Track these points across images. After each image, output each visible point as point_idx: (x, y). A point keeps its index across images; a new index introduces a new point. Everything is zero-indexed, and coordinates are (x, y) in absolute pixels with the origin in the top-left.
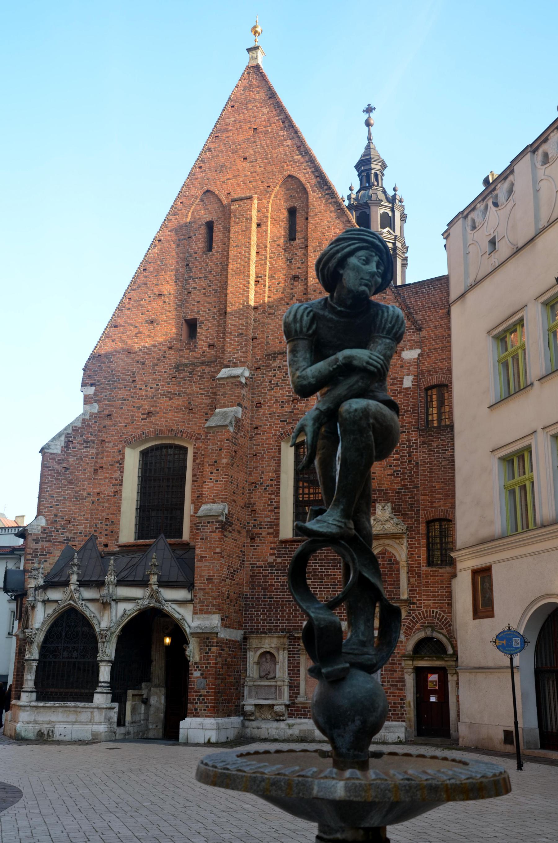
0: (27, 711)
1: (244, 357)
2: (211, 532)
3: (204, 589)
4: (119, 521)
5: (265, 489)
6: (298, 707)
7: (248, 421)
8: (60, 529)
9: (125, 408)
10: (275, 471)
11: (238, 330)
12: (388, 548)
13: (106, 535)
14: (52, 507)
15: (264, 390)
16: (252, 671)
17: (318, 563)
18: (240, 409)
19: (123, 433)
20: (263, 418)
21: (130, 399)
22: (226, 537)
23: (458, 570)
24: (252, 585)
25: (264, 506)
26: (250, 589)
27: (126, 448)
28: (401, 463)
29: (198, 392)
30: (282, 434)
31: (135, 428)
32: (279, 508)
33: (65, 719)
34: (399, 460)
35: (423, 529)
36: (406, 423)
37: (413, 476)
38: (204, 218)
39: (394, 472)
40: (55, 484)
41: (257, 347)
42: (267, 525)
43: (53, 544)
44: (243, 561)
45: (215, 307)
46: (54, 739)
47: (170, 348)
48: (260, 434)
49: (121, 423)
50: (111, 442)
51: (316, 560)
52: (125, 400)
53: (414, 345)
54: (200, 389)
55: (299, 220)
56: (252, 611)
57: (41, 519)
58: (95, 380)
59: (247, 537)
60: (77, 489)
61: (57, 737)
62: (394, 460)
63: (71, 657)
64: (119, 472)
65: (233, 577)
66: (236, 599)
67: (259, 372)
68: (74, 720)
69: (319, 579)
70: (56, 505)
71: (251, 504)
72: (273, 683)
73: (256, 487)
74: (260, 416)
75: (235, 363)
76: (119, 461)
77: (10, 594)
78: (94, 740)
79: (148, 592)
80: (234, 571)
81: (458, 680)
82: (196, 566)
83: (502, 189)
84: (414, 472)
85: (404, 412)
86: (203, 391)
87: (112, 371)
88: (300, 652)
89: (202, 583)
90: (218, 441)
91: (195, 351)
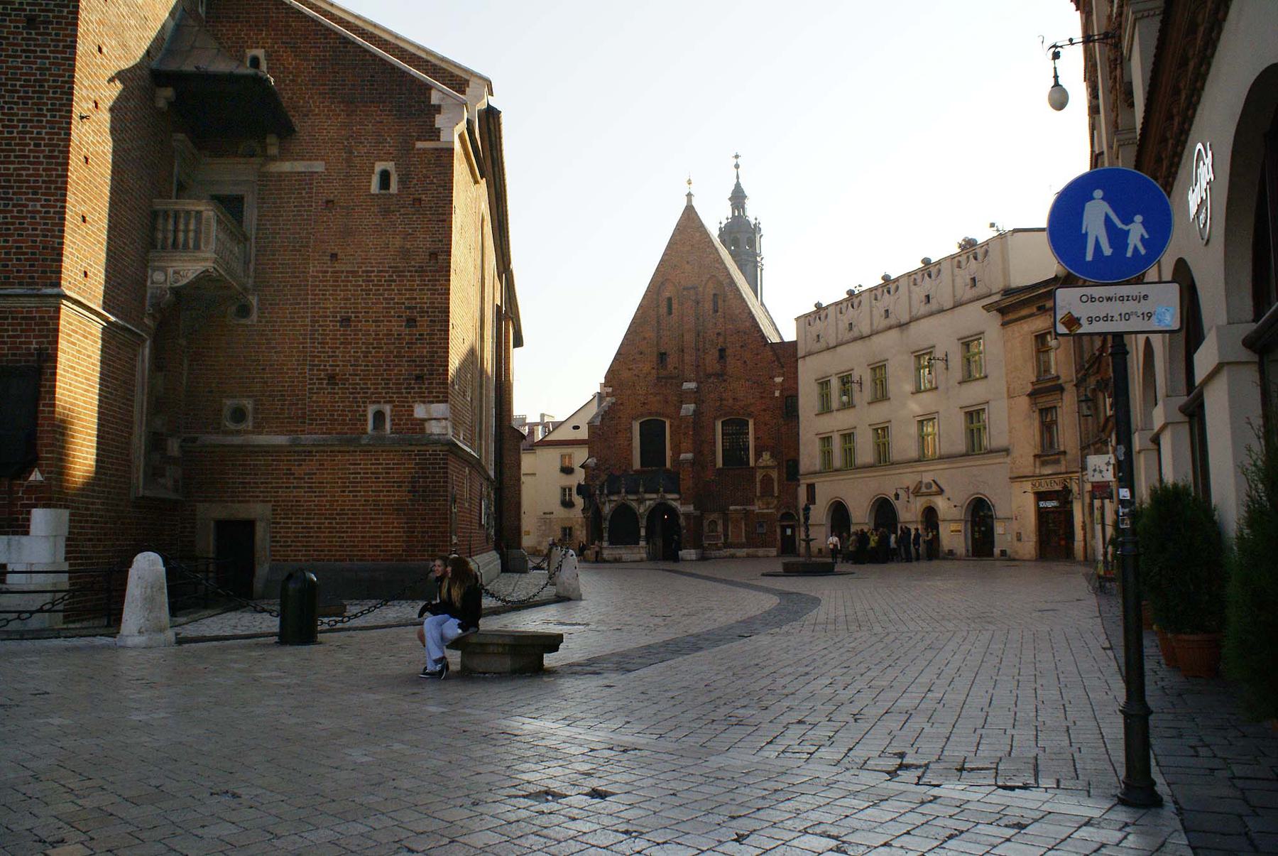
16: (706, 529)
35: (785, 465)
47: (653, 368)
55: (720, 302)
78: (642, 561)
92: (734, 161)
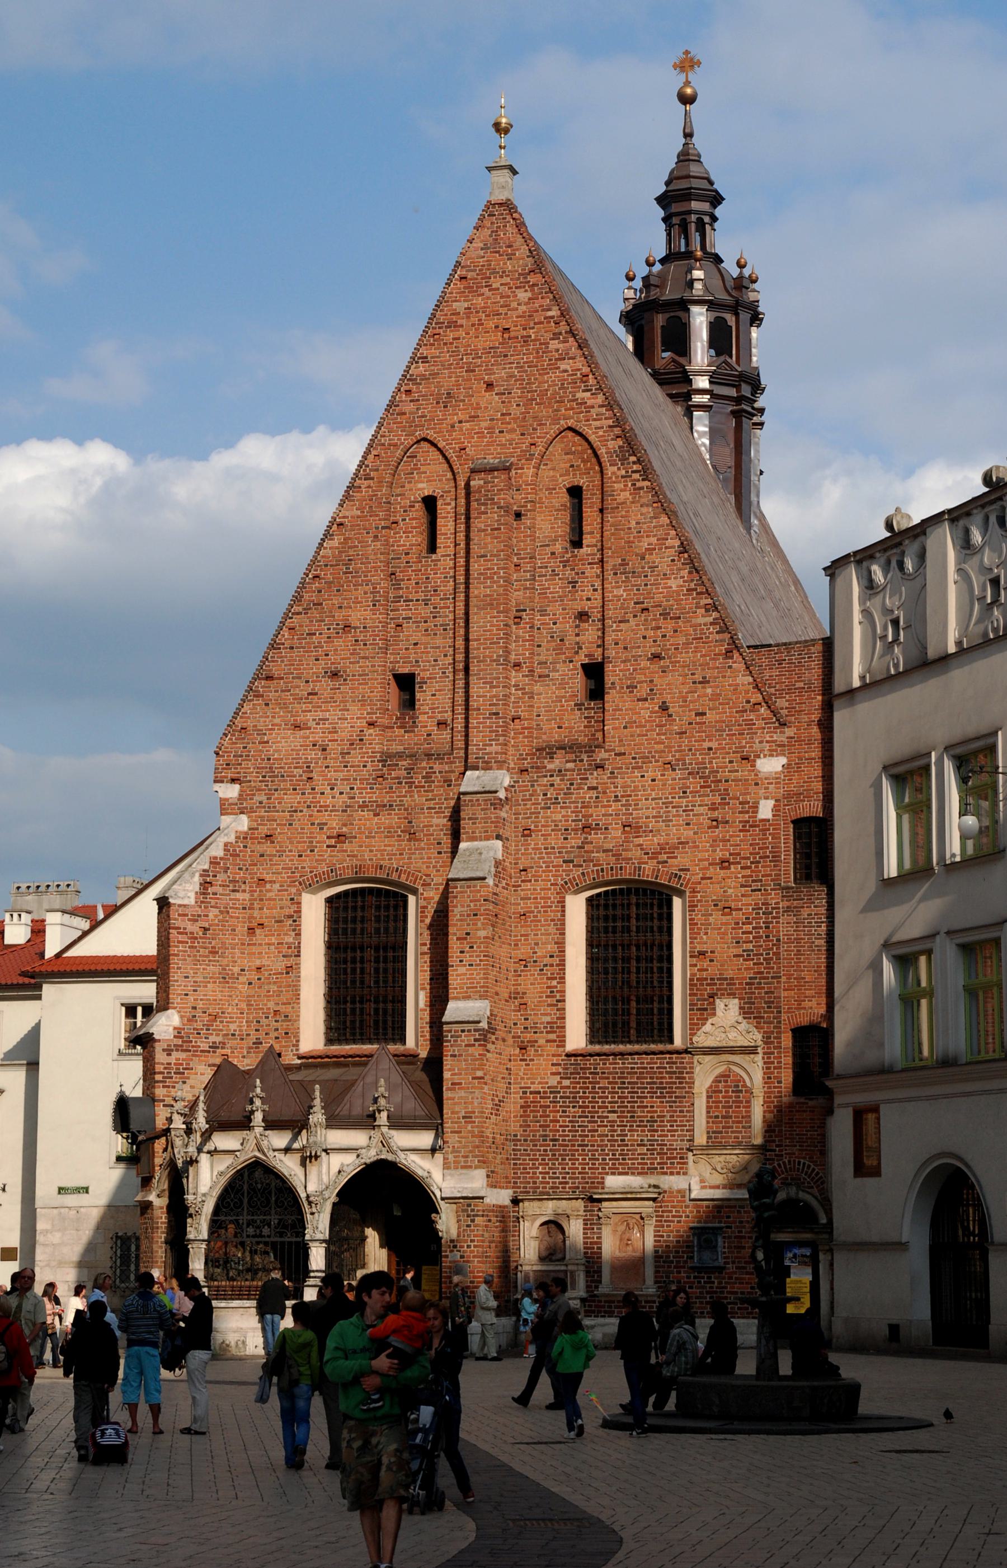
1: (502, 753)
2: (466, 1046)
3: (460, 1132)
4: (298, 1016)
5: (542, 970)
6: (600, 1301)
7: (511, 859)
9: (296, 824)
10: (556, 943)
11: (490, 705)
12: (734, 1068)
13: (277, 1038)
14: (187, 995)
15: (535, 808)
17: (627, 1088)
18: (499, 843)
19: (296, 868)
20: (535, 854)
21: (305, 810)
22: (488, 1051)
23: (835, 1105)
24: (525, 1121)
25: (540, 997)
26: (521, 1126)
27: (303, 894)
28: (754, 938)
29: (424, 804)
30: (566, 883)
31: (317, 860)
32: (564, 1001)
34: (751, 933)
35: (787, 1040)
36: (763, 876)
37: (772, 959)
38: (419, 490)
39: (744, 951)
40: (189, 956)
41: (521, 733)
42: (546, 1027)
44: (510, 1083)
45: (446, 656)
47: (371, 724)
48: (530, 881)
49: (291, 851)
50: (274, 882)
51: (624, 1083)
52: (296, 811)
53: (776, 750)
54: (427, 800)
56: (525, 1160)
57: (173, 1014)
58: (239, 773)
59: (513, 1046)
60: (225, 962)
62: (743, 933)
63: (261, 1236)
64: (293, 934)
65: (498, 1110)
66: (503, 1144)
67: (526, 777)
69: (628, 1112)
70: (195, 991)
71: (518, 993)
72: (563, 1268)
73: (525, 966)
74: (530, 851)
75: (487, 763)
76: (292, 916)
77: (125, 1135)
79: (376, 1134)
80: (500, 1101)
81: (832, 1259)
83: (911, 550)
84: (774, 954)
85: (760, 857)
86: (432, 804)
87: (269, 759)
88: (602, 1221)
89: (456, 1123)
90: (471, 901)
91: (413, 731)
92: (676, 81)
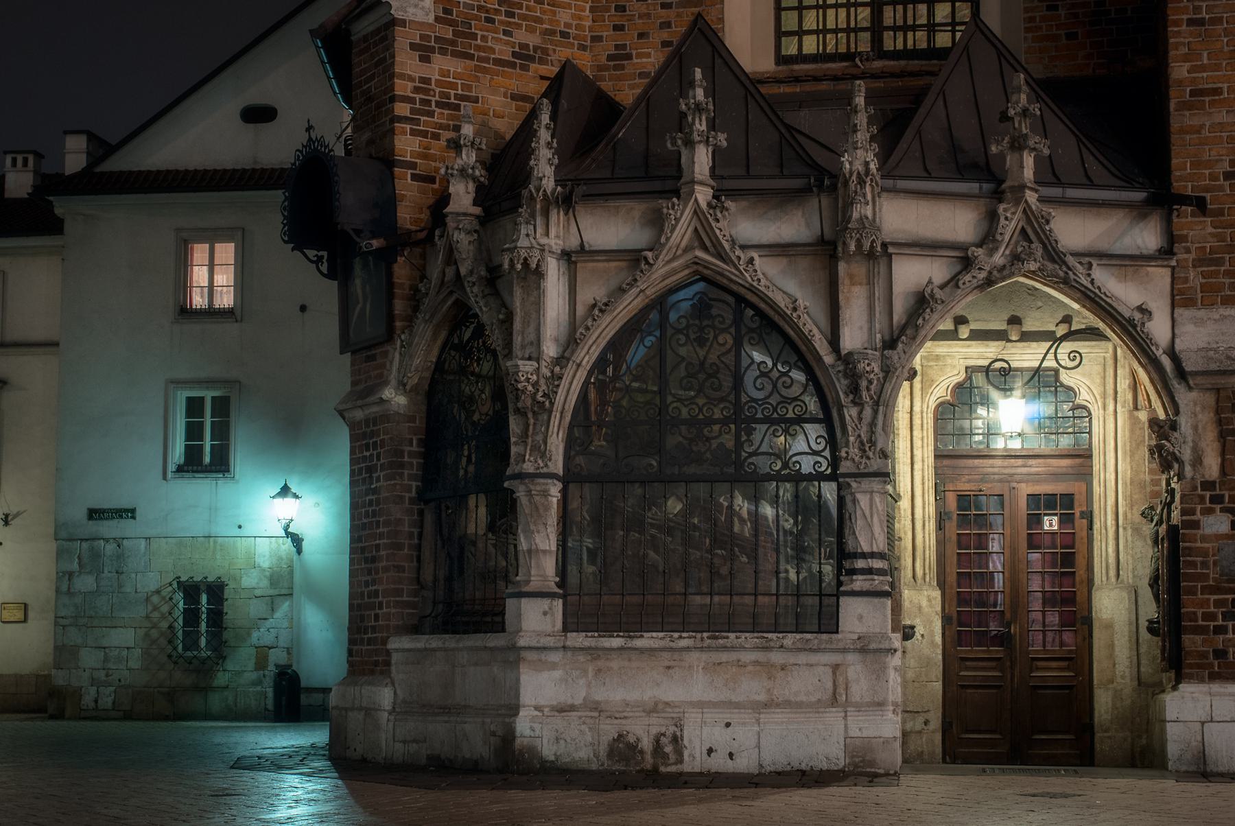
0: (553, 667)
8: (497, 12)
13: (665, 44)
33: (724, 695)
43: (478, 69)
46: (687, 767)
61: (694, 760)
68: (762, 697)
77: (311, 253)
82: (1175, 123)
